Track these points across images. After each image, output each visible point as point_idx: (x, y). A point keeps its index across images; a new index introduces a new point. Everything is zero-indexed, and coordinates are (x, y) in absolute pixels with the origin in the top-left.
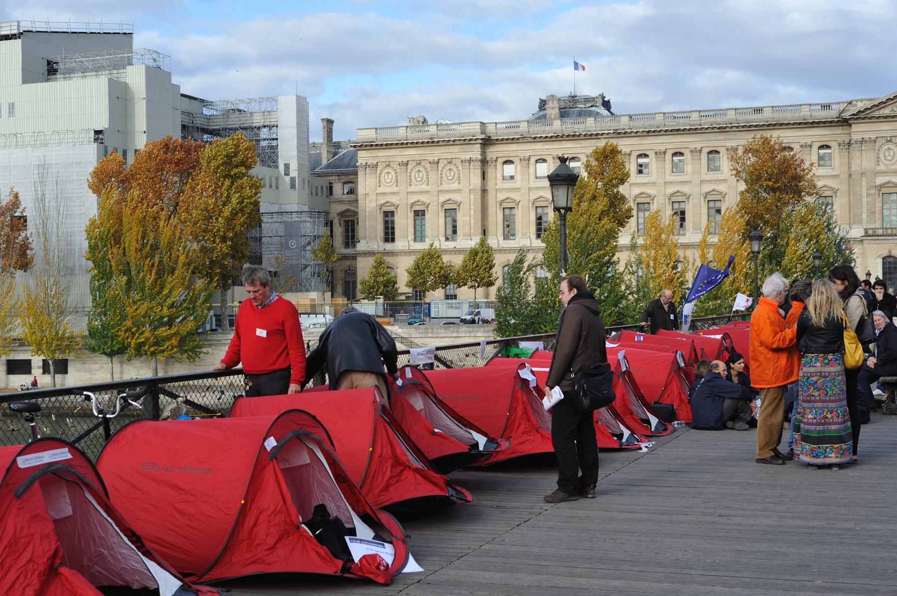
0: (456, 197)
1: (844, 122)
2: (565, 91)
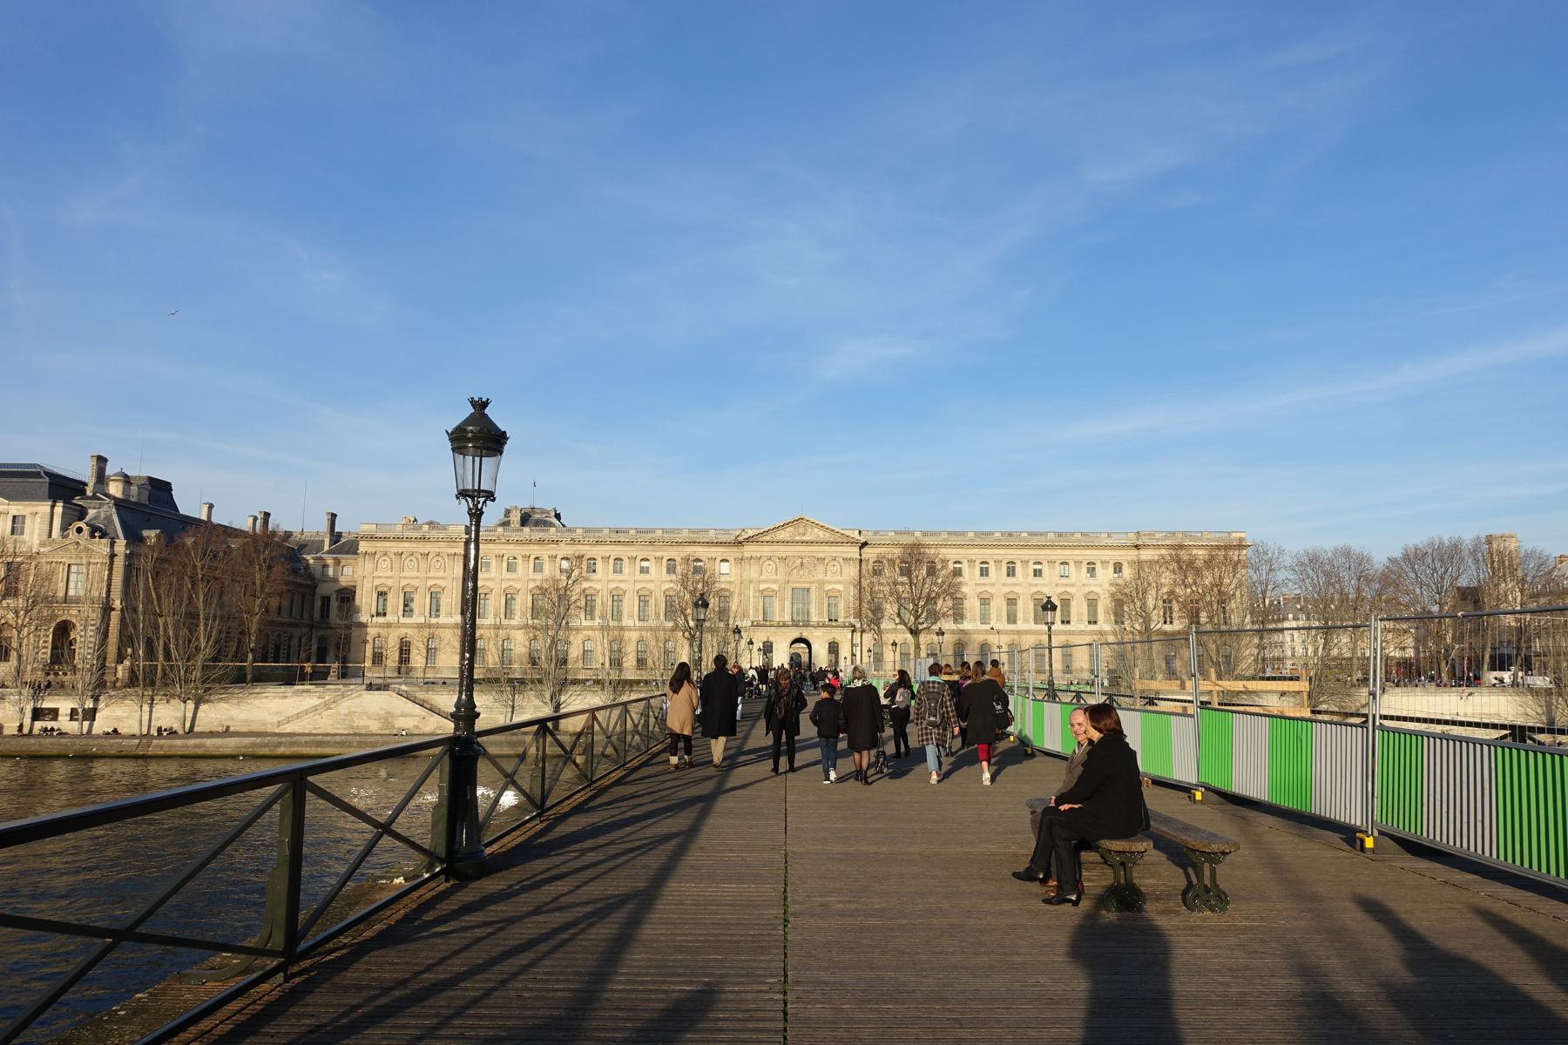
0: (442, 583)
2: (526, 504)
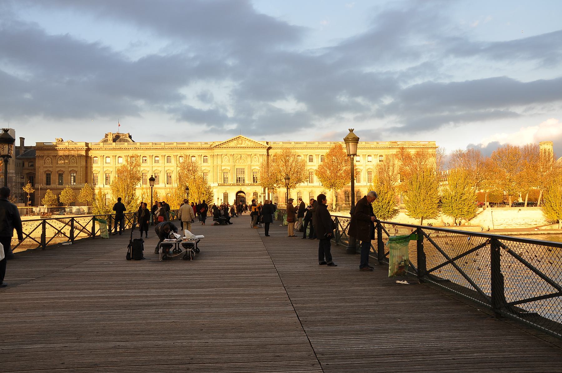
1: (211, 148)
